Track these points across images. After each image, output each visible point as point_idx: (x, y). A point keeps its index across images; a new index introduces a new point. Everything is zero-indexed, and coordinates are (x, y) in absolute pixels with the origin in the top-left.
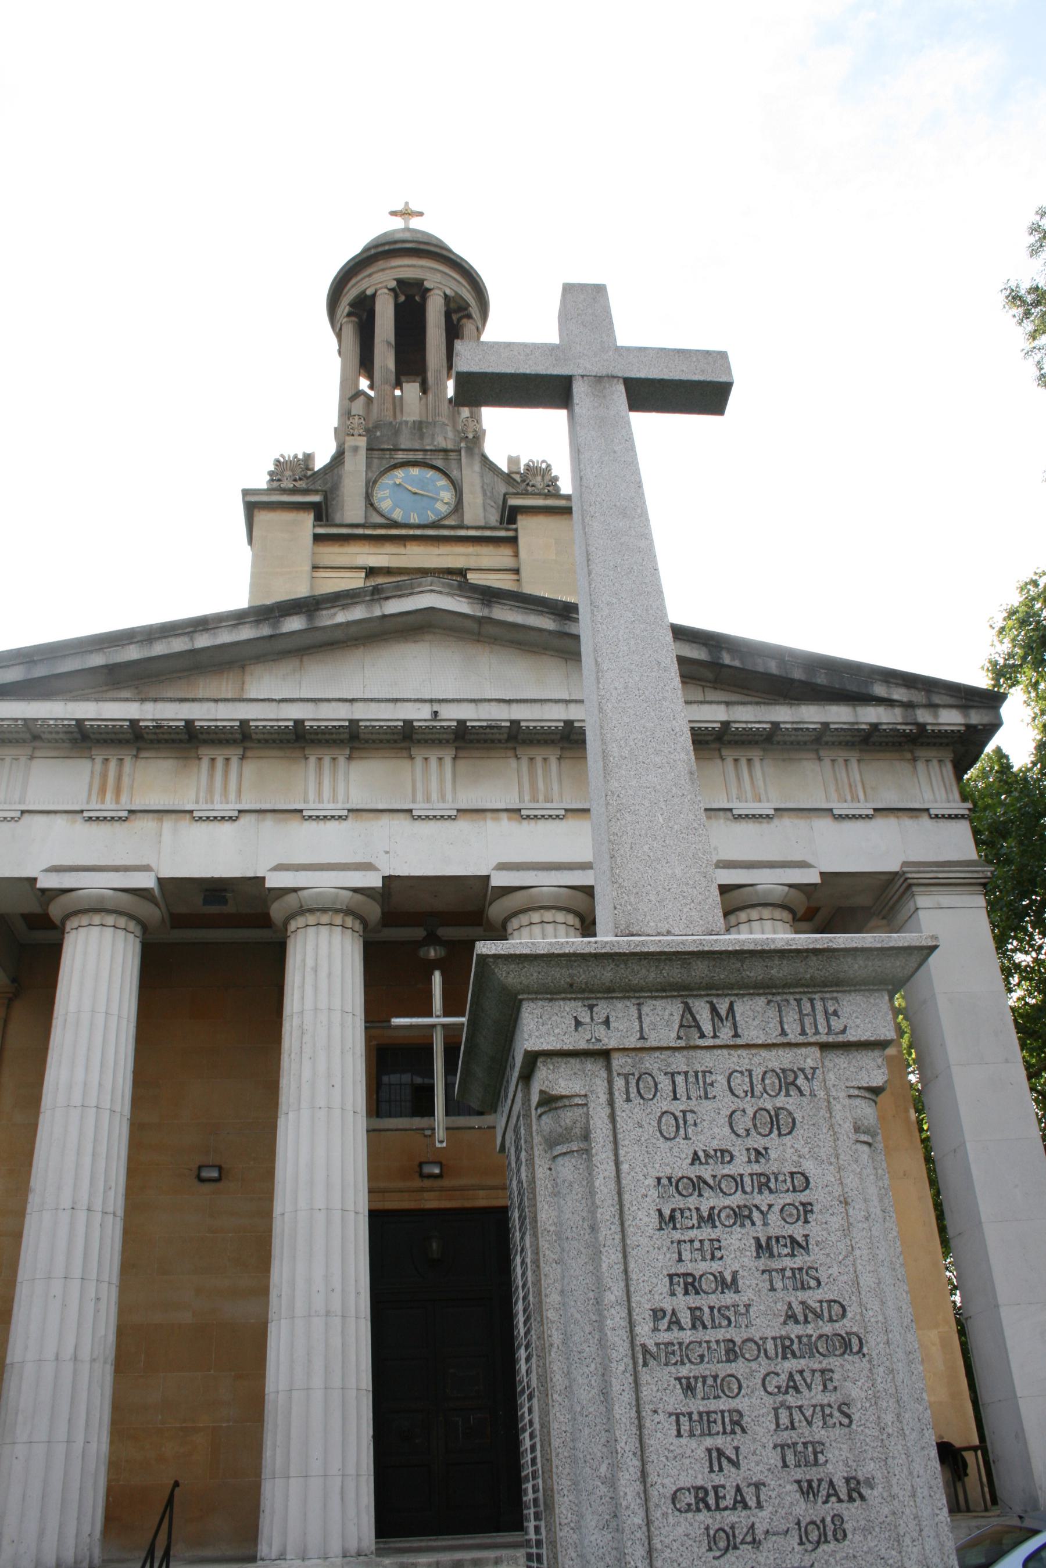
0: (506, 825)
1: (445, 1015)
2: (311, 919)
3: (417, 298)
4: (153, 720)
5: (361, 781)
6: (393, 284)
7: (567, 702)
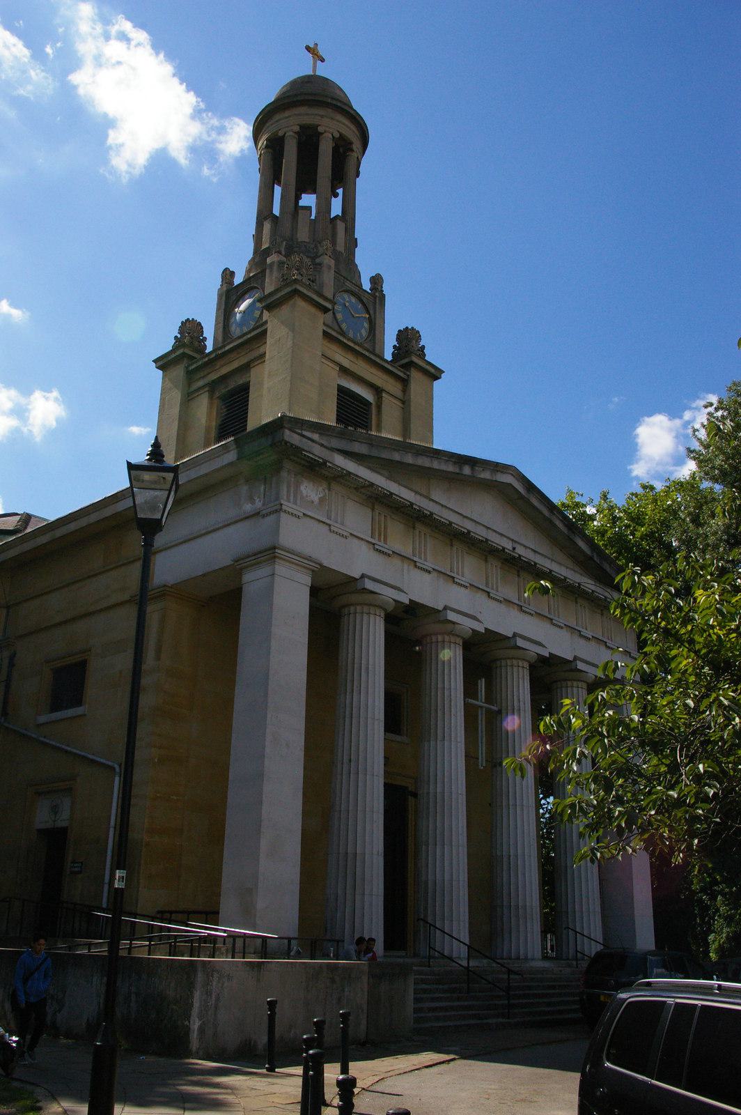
0: (515, 612)
1: (486, 703)
2: (453, 639)
3: (341, 150)
4: (419, 506)
5: (469, 567)
6: (337, 135)
7: (502, 535)
